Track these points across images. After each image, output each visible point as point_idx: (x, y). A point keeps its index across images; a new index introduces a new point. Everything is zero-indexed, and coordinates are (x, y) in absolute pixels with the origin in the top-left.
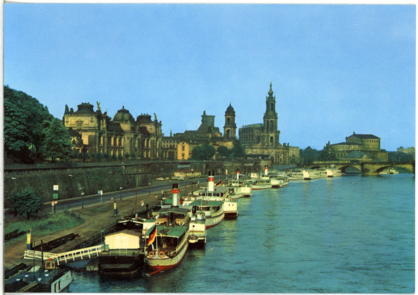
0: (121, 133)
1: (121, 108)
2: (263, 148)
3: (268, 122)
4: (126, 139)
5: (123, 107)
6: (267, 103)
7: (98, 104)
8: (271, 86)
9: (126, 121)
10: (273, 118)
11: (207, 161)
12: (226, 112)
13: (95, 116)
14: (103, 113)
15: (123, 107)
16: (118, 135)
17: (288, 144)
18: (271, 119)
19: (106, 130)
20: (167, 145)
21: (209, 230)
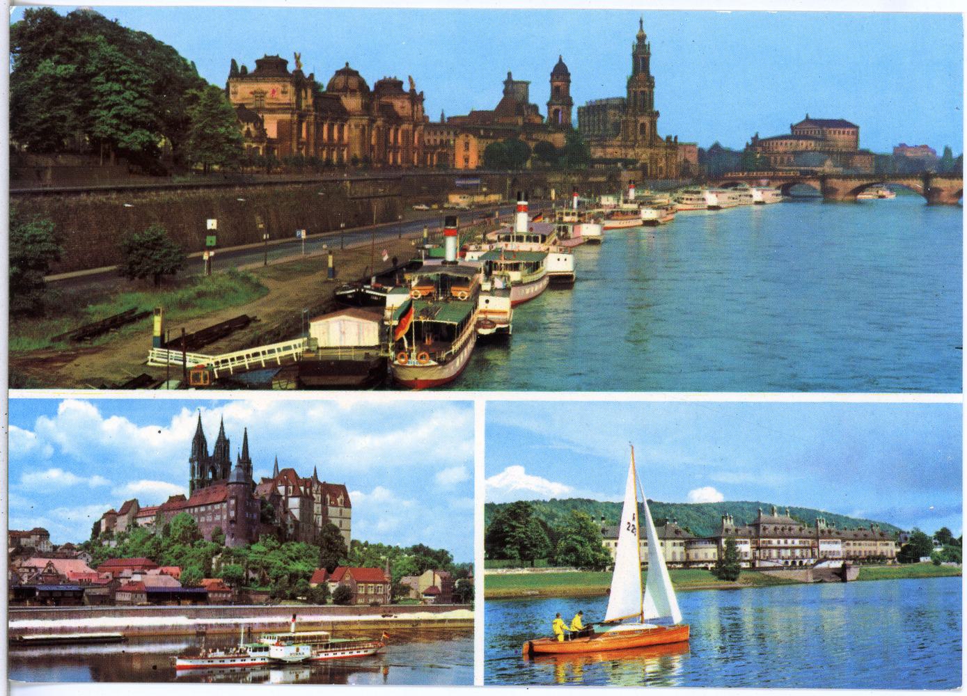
0: (342, 115)
1: (343, 66)
2: (625, 147)
3: (635, 92)
4: (353, 126)
5: (347, 64)
6: (635, 56)
7: (297, 58)
8: (641, 22)
9: (353, 92)
10: (645, 86)
11: (515, 172)
12: (552, 75)
13: (291, 82)
14: (307, 75)
15: (347, 64)
16: (336, 120)
17: (676, 138)
18: (642, 89)
19: (312, 109)
20: (435, 140)
21: (518, 310)
